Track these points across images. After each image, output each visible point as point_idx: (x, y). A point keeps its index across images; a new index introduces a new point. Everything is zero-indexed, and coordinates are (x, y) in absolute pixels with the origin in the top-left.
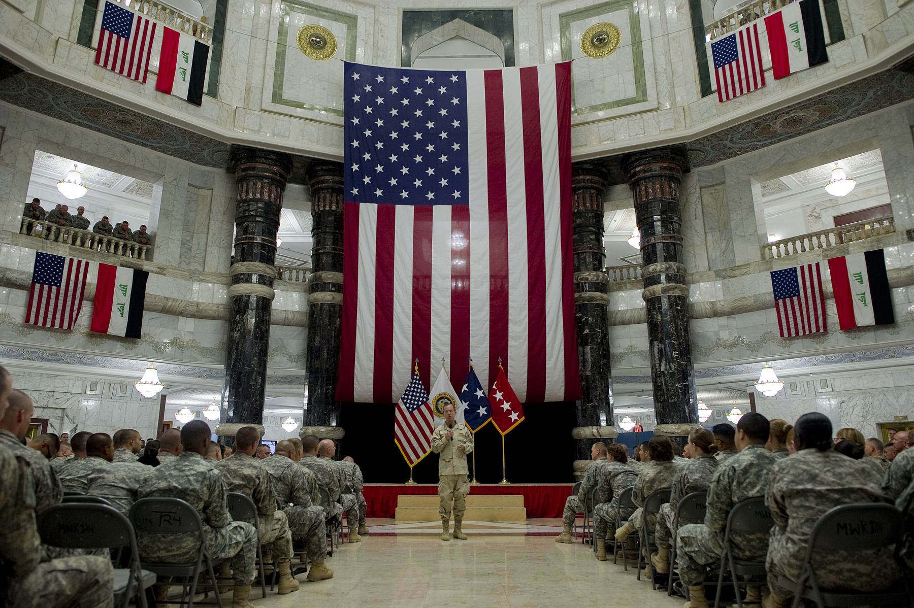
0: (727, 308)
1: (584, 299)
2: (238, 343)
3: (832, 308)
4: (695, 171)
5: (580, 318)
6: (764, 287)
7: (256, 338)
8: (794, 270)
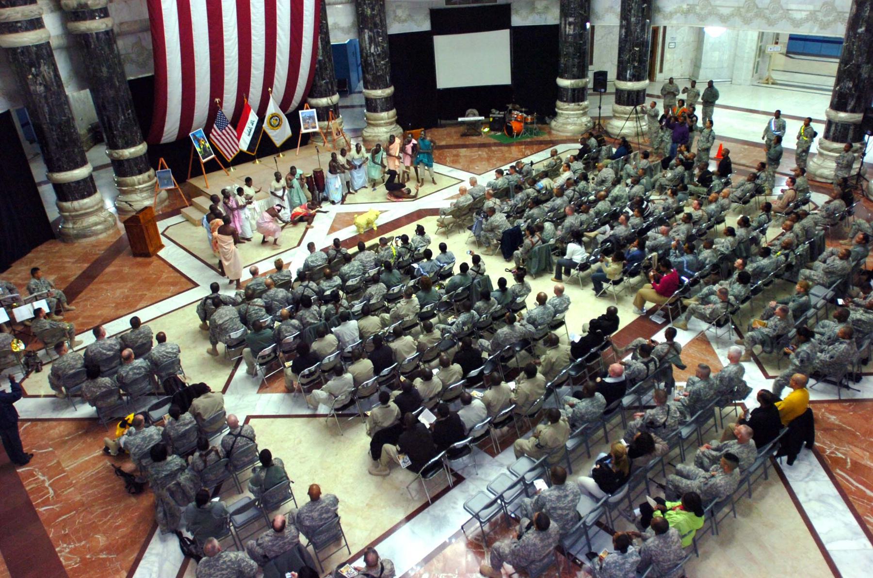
2: (45, 97)
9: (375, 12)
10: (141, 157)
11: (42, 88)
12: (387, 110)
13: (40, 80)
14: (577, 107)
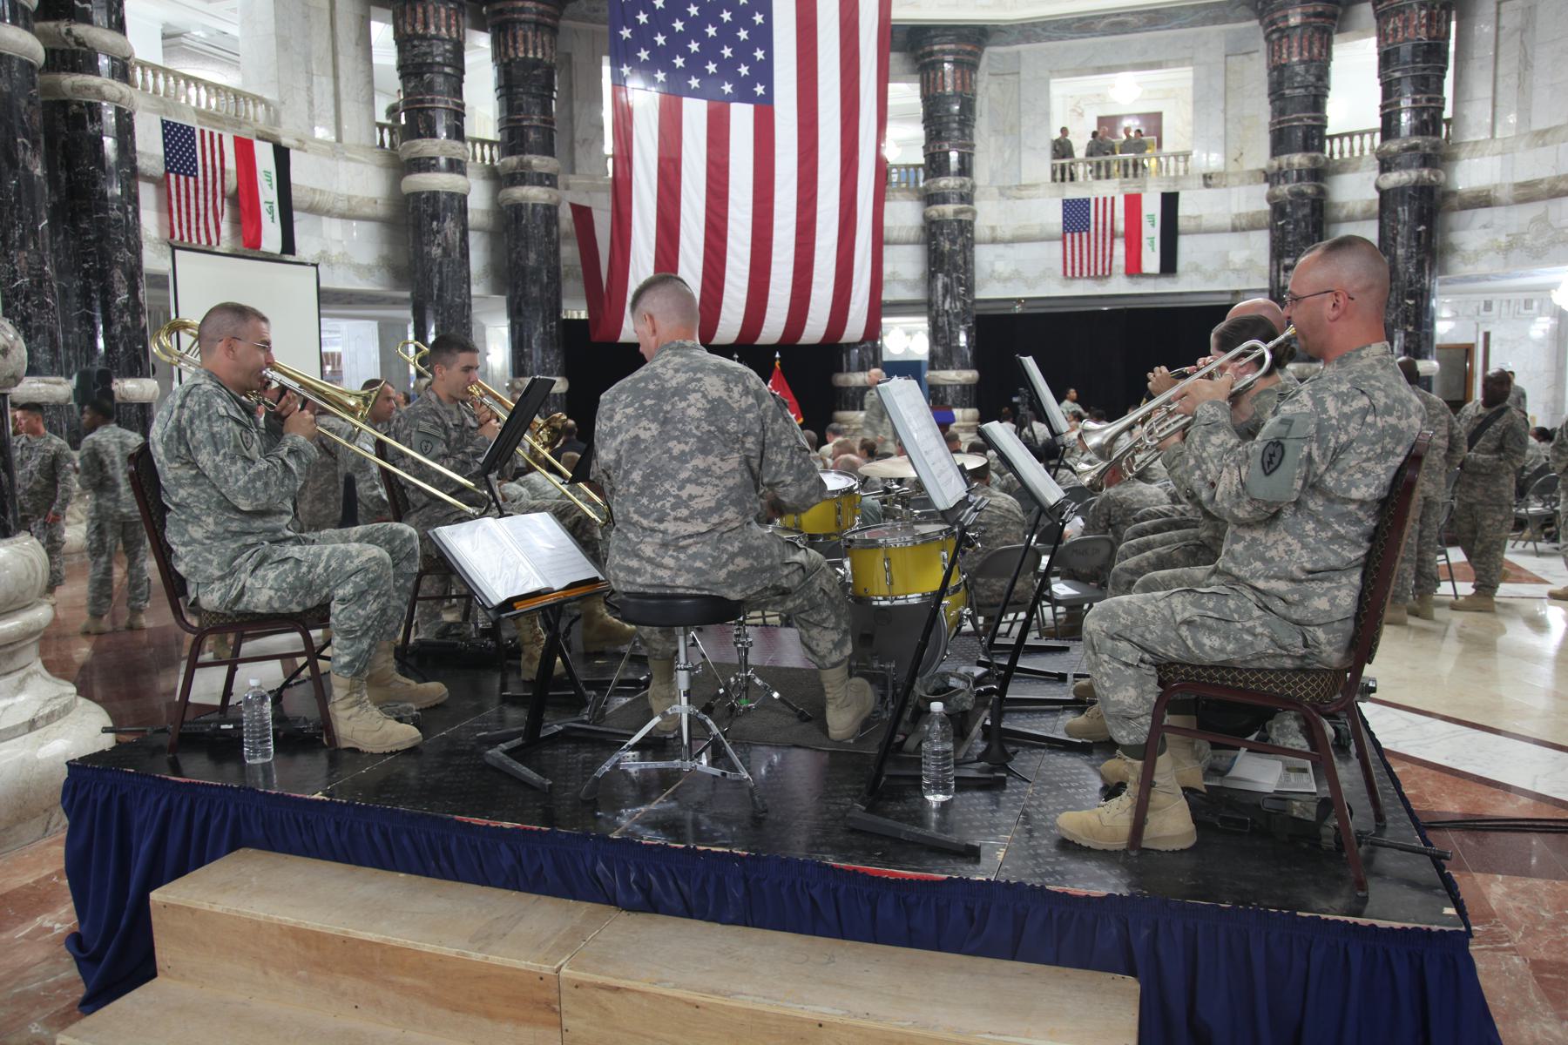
0: (1008, 235)
3: (1120, 248)
4: (988, 50)
6: (1053, 217)
8: (1087, 201)
9: (957, 247)
11: (439, 251)
13: (439, 238)
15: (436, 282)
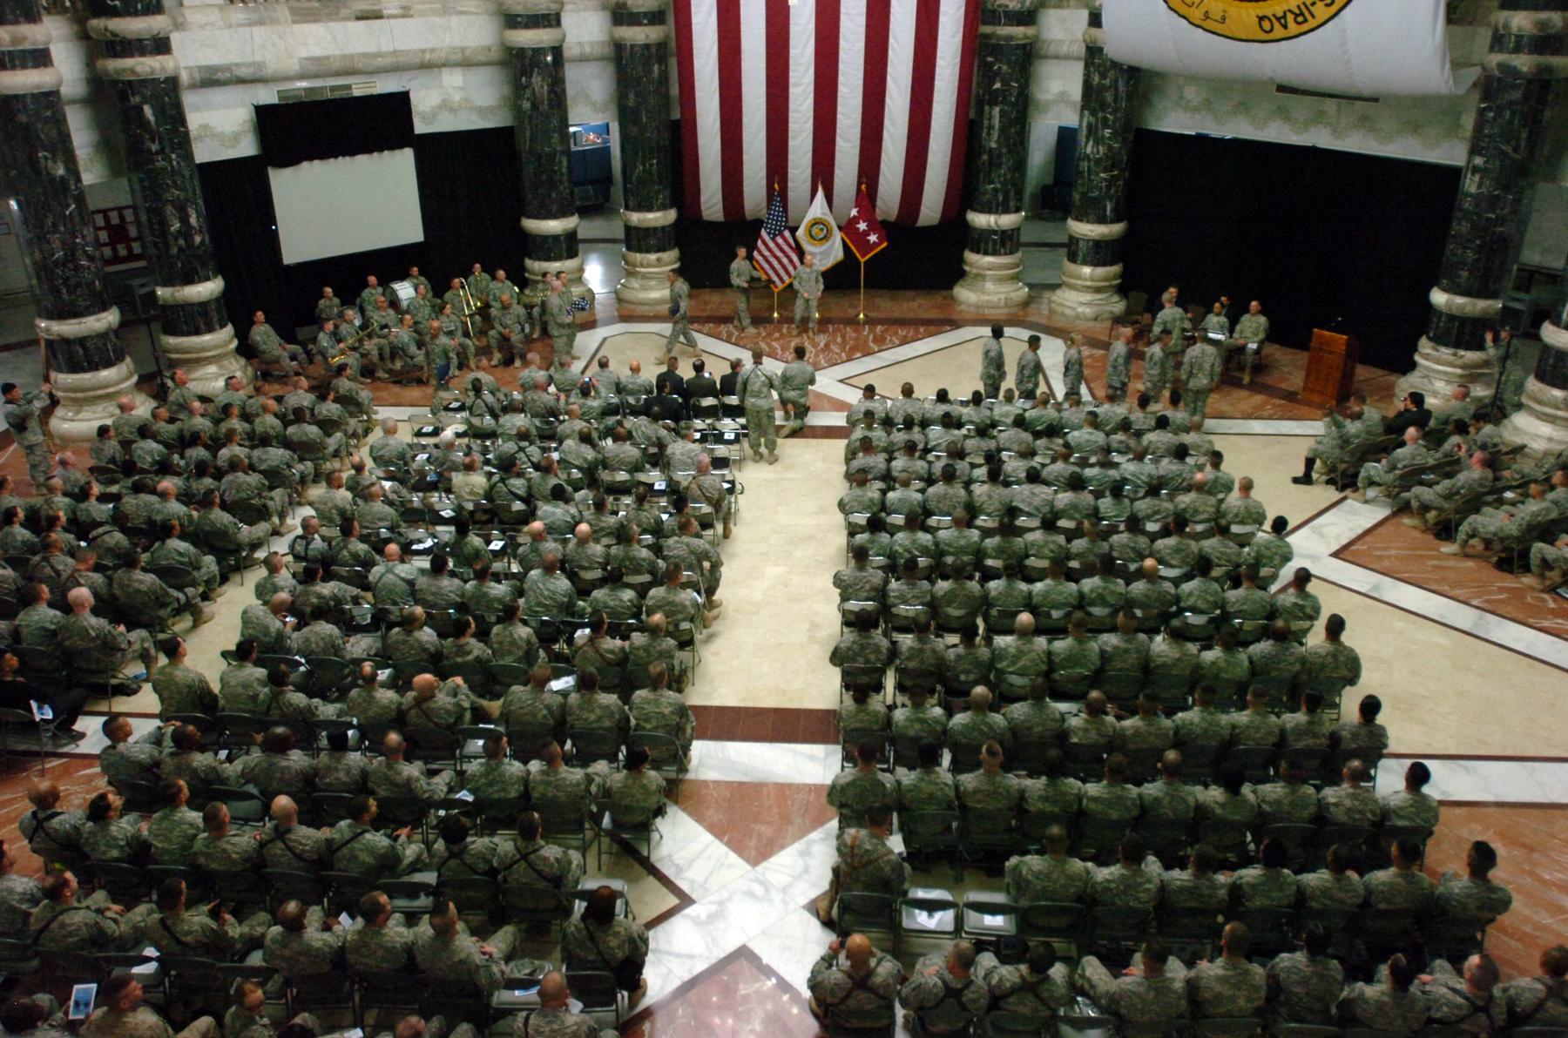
1: (1000, 38)
5: (992, 64)
7: (551, 106)
9: (1107, 82)
10: (655, 229)
12: (1096, 263)
13: (528, 93)
14: (1452, 358)
15: (528, 133)
